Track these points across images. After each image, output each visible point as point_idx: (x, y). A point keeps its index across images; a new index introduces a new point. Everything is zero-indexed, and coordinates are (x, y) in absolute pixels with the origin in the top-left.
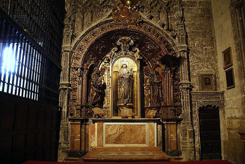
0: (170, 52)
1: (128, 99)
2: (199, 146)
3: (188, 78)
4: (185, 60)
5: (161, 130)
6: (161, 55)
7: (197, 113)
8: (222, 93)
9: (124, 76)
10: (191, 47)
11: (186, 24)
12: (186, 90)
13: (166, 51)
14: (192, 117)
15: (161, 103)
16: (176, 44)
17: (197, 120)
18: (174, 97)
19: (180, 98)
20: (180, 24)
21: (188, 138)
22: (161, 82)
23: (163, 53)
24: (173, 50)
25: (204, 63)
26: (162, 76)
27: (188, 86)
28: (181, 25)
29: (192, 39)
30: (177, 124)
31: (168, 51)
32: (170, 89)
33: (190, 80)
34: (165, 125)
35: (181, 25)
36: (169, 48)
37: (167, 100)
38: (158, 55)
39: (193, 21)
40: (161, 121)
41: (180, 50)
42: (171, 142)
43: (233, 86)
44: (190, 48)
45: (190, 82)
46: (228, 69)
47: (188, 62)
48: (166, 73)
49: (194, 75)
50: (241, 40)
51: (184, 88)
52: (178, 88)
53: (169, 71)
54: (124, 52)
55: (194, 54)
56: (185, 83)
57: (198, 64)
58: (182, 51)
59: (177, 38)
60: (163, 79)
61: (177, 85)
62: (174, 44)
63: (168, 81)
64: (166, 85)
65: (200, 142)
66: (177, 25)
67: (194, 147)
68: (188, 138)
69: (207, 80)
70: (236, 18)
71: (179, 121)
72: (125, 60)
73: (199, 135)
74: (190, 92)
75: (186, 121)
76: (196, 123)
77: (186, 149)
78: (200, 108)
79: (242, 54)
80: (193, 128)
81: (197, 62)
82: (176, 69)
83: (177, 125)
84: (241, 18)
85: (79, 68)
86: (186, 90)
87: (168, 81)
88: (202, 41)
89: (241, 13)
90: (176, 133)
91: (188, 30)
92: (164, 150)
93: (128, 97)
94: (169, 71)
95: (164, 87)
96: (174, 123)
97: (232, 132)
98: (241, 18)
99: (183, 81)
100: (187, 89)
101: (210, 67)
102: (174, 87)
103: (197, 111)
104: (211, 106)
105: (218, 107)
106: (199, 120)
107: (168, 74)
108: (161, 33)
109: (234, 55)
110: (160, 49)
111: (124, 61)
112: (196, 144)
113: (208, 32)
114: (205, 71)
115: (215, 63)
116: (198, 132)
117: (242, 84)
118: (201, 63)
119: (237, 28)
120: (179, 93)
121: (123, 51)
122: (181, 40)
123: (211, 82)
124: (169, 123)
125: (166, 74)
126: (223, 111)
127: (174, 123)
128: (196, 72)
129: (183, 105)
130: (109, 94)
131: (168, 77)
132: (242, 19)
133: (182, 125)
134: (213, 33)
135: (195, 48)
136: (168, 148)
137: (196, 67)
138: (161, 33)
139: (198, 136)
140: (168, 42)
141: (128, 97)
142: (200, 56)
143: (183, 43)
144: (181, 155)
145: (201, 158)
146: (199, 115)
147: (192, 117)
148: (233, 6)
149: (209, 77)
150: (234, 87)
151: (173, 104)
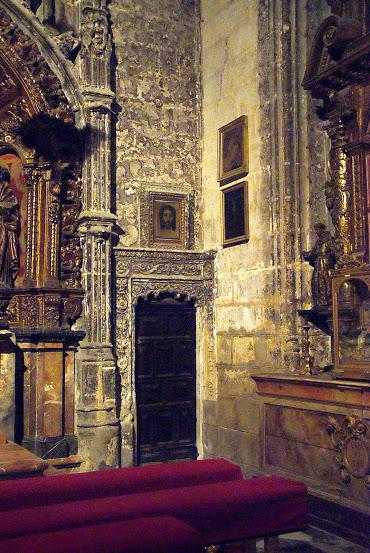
0: (55, 107)
2: (133, 420)
3: (107, 201)
4: (104, 140)
5: (14, 370)
6: (21, 113)
7: (130, 315)
8: (210, 258)
10: (125, 101)
11: (114, 15)
12: (101, 242)
13: (42, 102)
14: (113, 327)
15: (13, 280)
16: (76, 80)
17: (130, 337)
18: (59, 260)
19: (80, 266)
20: (94, 11)
21: (99, 394)
22: (18, 207)
23: (30, 106)
24: (65, 101)
25: (159, 158)
26: (23, 189)
27: (108, 229)
28: (97, 14)
29: (131, 73)
30: (64, 350)
31: (46, 103)
32: (46, 235)
33: (113, 210)
34: (26, 354)
35: (97, 14)
36: (51, 91)
37: (35, 269)
39: (138, 8)
40: (13, 339)
41: (91, 105)
42: (44, 409)
43: (242, 238)
44: (120, 103)
45: (113, 216)
46: (234, 183)
47: (113, 148)
48: (36, 177)
49: (130, 192)
51: (93, 234)
52: (76, 231)
53: (49, 173)
55: (134, 126)
56: (99, 219)
57: (141, 158)
58: (94, 109)
59: (79, 61)
60: (25, 196)
61: (70, 221)
62: (69, 80)
63: (43, 205)
64: (36, 220)
65: (134, 406)
66: (83, 12)
67: (118, 424)
68: (99, 394)
69: (168, 212)
70: (272, 23)
71: (71, 341)
73: (134, 386)
74: (111, 246)
75: (95, 341)
76: (124, 348)
77: (92, 430)
78: (140, 299)
79: (277, 141)
80: (116, 365)
81: (139, 151)
82: (71, 167)
83: (65, 355)
84: (286, 28)
86: (101, 242)
87: (43, 205)
88: (161, 84)
89: (289, 12)
90: (61, 381)
91: (118, 39)
92: (19, 438)
94: (49, 173)
95: (26, 224)
96: (55, 346)
97: (231, 374)
98: (286, 28)
99: (93, 212)
100: (105, 236)
101: (179, 172)
102: (61, 226)
103: (129, 310)
104: (173, 295)
105: (193, 300)
106: (136, 338)
107: (44, 182)
108: (27, 32)
109: (254, 142)
110: (19, 91)
112: (123, 412)
113: (182, 57)
114: (161, 183)
115: (193, 160)
116: (129, 377)
117: (270, 233)
118: (152, 157)
119: (271, 56)
120: (77, 248)
122: (95, 68)
123: (177, 220)
124: (40, 346)
125: (38, 182)
126: (208, 311)
127: (55, 346)
128: (136, 184)
129: (89, 289)
131: (44, 193)
132: (289, 32)
133: (80, 355)
134: (197, 61)
135: (137, 105)
136: (32, 432)
137: (135, 169)
138: (27, 32)
139: (129, 388)
140: (49, 68)
142: (151, 132)
143: (99, 81)
144: (75, 451)
145: (138, 458)
146: (137, 324)
147: (113, 327)
149: (172, 205)
150: (246, 241)
151: (55, 284)
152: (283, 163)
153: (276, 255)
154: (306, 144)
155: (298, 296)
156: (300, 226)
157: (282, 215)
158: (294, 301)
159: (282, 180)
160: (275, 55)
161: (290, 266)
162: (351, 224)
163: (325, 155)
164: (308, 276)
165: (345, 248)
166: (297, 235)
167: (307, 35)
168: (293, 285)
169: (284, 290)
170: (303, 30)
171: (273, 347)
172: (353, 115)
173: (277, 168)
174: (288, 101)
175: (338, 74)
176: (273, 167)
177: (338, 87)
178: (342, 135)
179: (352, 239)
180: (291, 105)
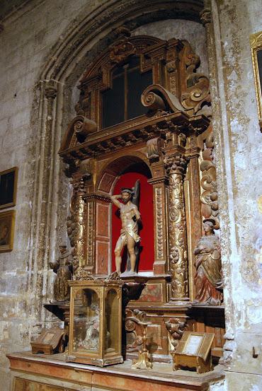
43: (5, 247)
50: (43, 159)
70: (40, 114)
79: (38, 186)
84: (49, 118)
89: (52, 109)
98: (49, 118)
117: (28, 248)
119: (39, 133)
132: (51, 120)
148: (40, 89)
150: (10, 251)
152: (41, 201)
153: (31, 263)
154: (57, 191)
155: (44, 293)
156: (49, 244)
157: (37, 236)
158: (41, 297)
159: (39, 212)
160: (41, 132)
161: (40, 272)
162: (85, 246)
163: (68, 199)
164: (52, 280)
165: (80, 263)
166: (46, 251)
167: (62, 125)
168: (41, 285)
169: (35, 289)
170: (60, 122)
171: (22, 330)
172: (90, 177)
173: (37, 204)
174: (48, 162)
175: (82, 150)
176: (34, 203)
177: (82, 159)
178: (82, 188)
179: (85, 257)
180: (49, 165)
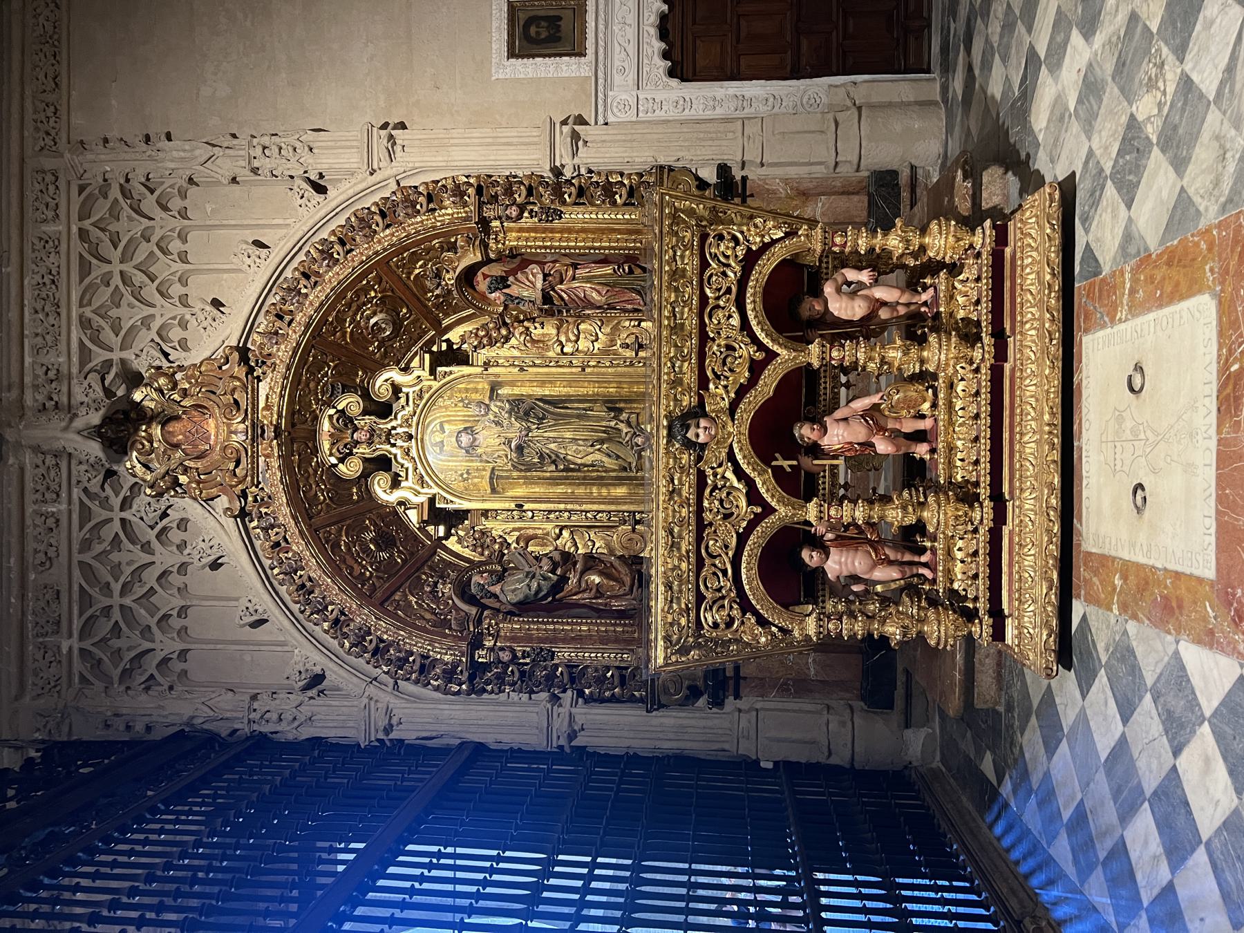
1: (622, 426)
9: (513, 445)
38: (410, 273)
54: (399, 443)
69: (533, 30)
72: (438, 437)
85: (472, 656)
93: (612, 424)
111: (442, 442)
121: (394, 445)
123: (542, 13)
130: (599, 512)
141: (612, 424)
149: (522, 23)
